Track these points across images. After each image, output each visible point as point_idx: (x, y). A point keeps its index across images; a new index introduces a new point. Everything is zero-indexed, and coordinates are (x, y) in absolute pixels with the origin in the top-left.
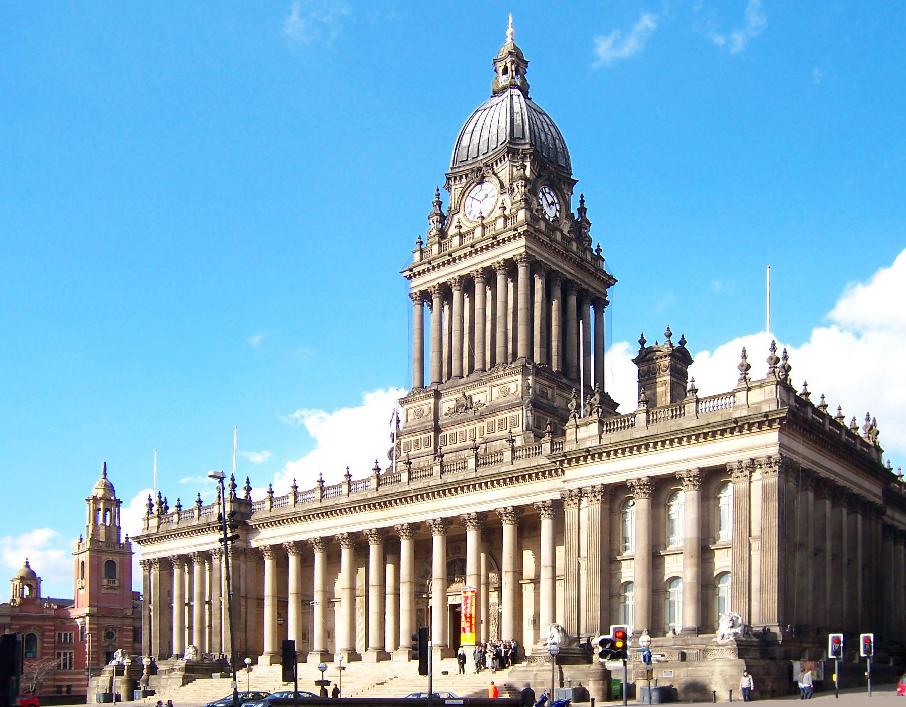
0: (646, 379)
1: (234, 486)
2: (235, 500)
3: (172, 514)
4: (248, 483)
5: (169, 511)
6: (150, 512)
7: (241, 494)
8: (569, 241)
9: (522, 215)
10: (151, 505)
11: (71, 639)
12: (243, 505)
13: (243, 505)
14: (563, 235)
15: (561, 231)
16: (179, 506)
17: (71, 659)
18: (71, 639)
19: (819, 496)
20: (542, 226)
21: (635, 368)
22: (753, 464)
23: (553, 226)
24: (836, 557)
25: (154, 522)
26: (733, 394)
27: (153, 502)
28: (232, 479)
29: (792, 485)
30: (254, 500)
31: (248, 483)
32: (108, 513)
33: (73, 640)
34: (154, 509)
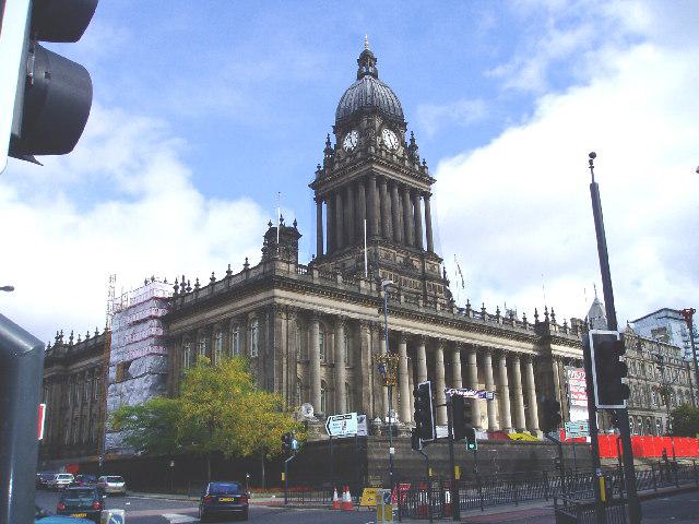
8: (403, 160)
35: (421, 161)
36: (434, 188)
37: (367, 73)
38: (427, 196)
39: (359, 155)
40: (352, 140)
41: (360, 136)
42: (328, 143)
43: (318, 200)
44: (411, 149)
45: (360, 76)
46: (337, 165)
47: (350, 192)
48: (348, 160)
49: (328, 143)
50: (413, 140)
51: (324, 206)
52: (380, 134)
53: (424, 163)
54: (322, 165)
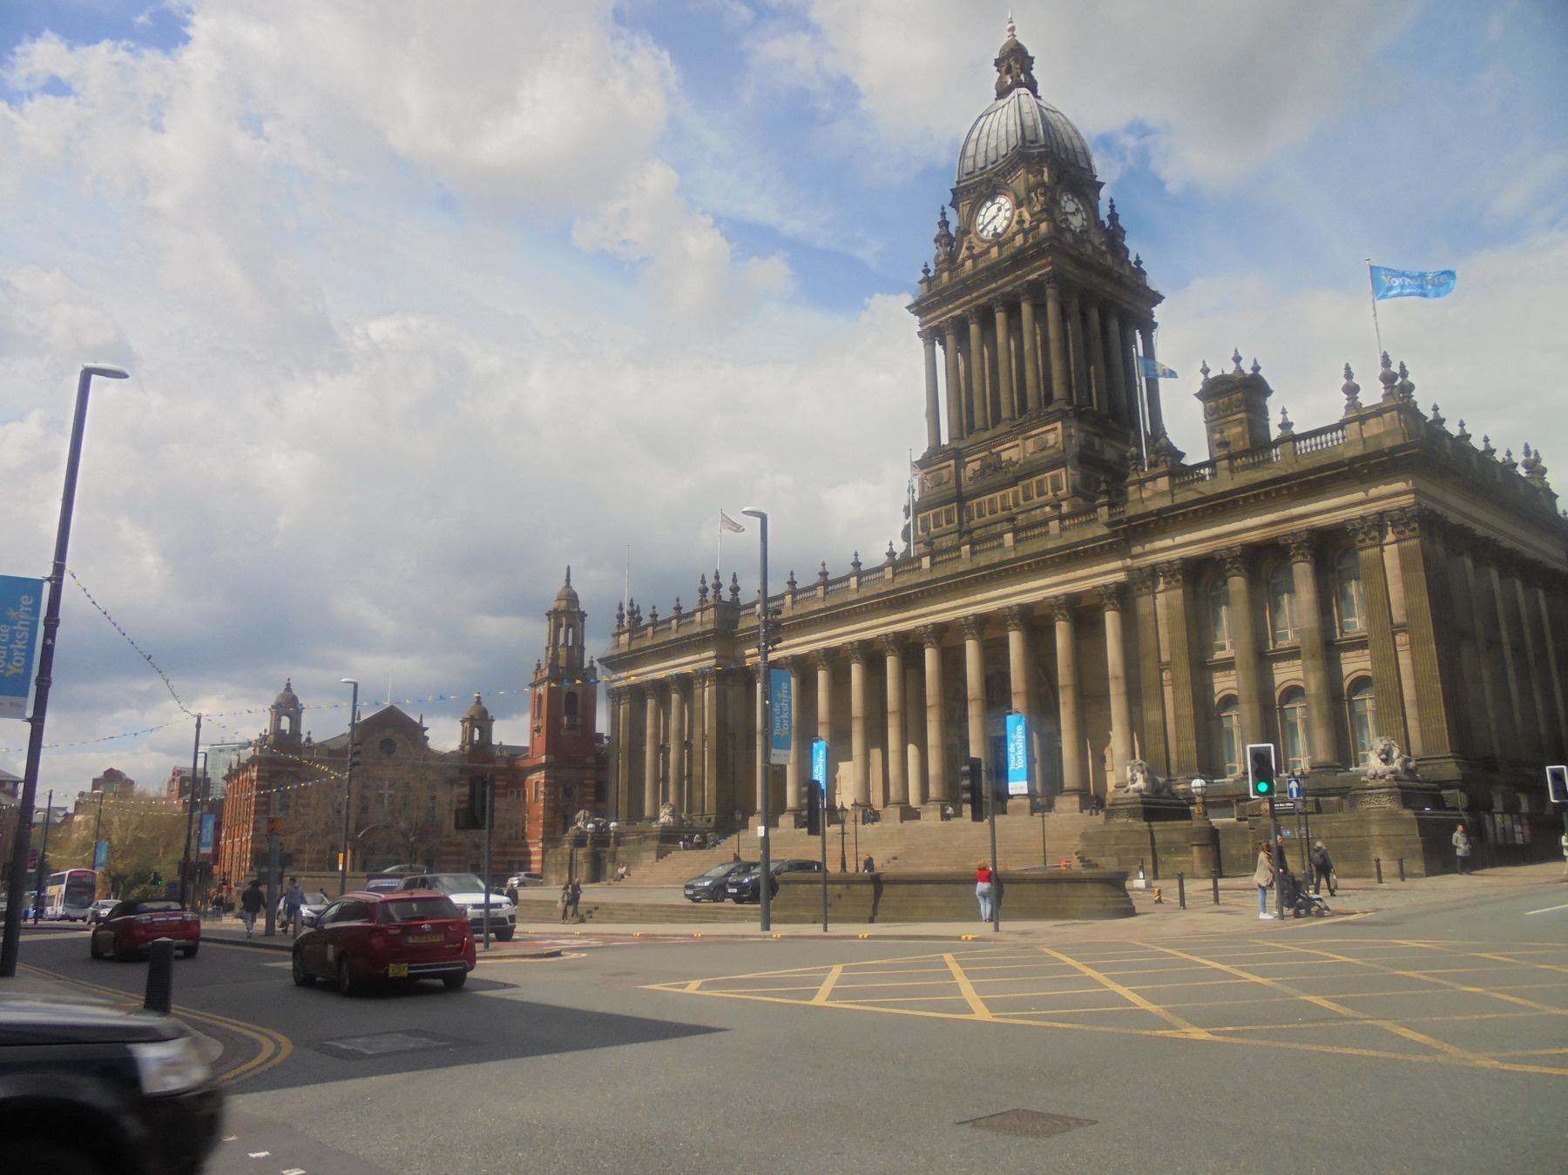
0: (1215, 419)
1: (718, 586)
2: (720, 606)
3: (646, 627)
4: (735, 580)
5: (643, 623)
6: (621, 625)
7: (726, 595)
8: (1103, 254)
9: (1043, 226)
14: (1095, 248)
15: (1092, 244)
16: (654, 616)
19: (1479, 563)
20: (1069, 238)
21: (1199, 406)
22: (1379, 523)
23: (1081, 237)
24: (1519, 650)
25: (624, 638)
26: (1341, 426)
28: (717, 577)
29: (1439, 548)
30: (742, 602)
35: (1132, 258)
36: (1158, 311)
37: (1020, 85)
38: (1148, 327)
39: (1019, 239)
40: (997, 216)
41: (1018, 204)
42: (944, 224)
43: (932, 335)
44: (1114, 235)
45: (1002, 92)
46: (969, 263)
47: (1000, 317)
48: (994, 252)
49: (944, 224)
50: (1113, 217)
51: (939, 349)
52: (1057, 203)
53: (1138, 262)
54: (932, 267)
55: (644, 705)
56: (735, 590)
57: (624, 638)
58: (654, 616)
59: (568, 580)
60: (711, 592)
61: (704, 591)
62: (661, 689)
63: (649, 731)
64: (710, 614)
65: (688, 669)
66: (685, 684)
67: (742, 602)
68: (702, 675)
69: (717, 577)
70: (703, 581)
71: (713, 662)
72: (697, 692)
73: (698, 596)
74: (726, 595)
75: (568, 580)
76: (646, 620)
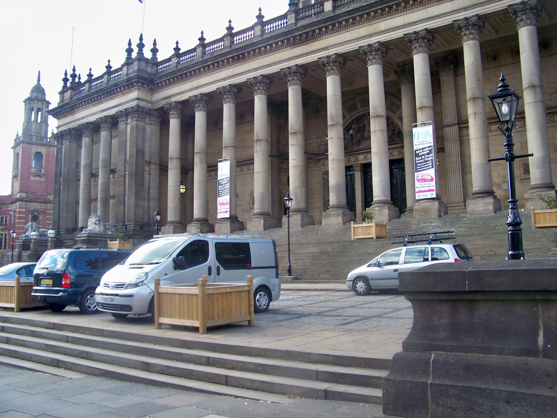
1: (141, 46)
4: (155, 44)
6: (65, 86)
7: (148, 54)
10: (66, 80)
11: (6, 221)
12: (150, 65)
13: (150, 65)
16: (90, 75)
17: (5, 239)
18: (6, 221)
27: (68, 77)
28: (141, 39)
31: (155, 44)
32: (40, 113)
33: (8, 223)
34: (69, 84)
55: (80, 147)
56: (155, 51)
57: (68, 94)
58: (90, 75)
59: (39, 80)
60: (136, 50)
61: (129, 51)
62: (94, 128)
63: (83, 163)
64: (135, 66)
65: (113, 112)
66: (113, 122)
67: (159, 60)
68: (126, 113)
69: (141, 39)
70: (130, 44)
71: (135, 103)
72: (122, 126)
73: (125, 55)
74: (148, 54)
75: (39, 80)
76: (84, 79)
